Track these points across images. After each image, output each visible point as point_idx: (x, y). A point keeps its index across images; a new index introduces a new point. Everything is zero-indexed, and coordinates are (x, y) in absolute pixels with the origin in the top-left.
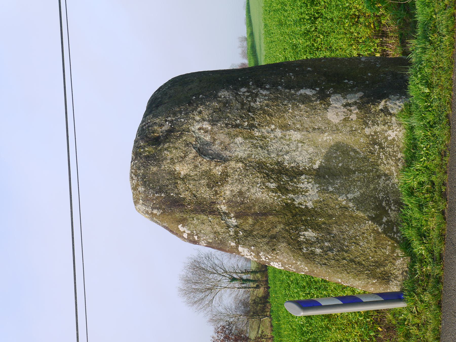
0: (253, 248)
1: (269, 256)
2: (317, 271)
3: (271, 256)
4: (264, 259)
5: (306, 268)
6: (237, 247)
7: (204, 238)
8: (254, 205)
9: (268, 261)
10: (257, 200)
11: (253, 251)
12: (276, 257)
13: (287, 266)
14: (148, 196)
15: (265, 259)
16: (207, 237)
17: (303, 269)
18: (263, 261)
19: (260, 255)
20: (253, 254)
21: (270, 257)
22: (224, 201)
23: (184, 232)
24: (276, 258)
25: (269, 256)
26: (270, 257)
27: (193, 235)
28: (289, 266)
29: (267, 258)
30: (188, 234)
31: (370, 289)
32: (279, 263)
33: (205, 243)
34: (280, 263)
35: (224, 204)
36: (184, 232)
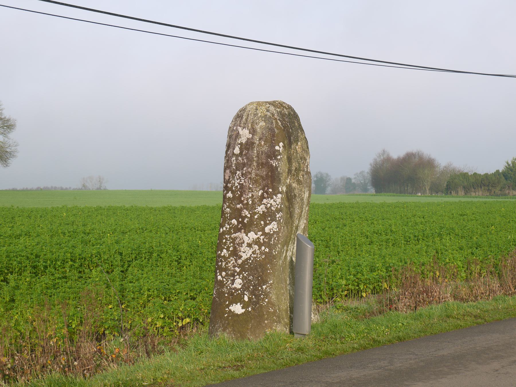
0: (282, 206)
1: (282, 220)
2: (276, 262)
3: (282, 222)
4: (278, 216)
5: (276, 253)
6: (280, 193)
7: (280, 165)
8: (292, 208)
9: (278, 219)
10: (294, 209)
11: (281, 207)
12: (282, 226)
13: (275, 236)
14: (285, 117)
15: (279, 217)
16: (280, 167)
17: (275, 250)
18: (276, 215)
19: (280, 212)
20: (279, 207)
21: (281, 221)
22: (291, 182)
23: (280, 147)
24: (281, 226)
25: (282, 220)
26: (281, 221)
27: (280, 155)
28: (275, 238)
29: (280, 218)
30: (279, 150)
31: (271, 309)
32: (277, 229)
33: (276, 164)
34: (278, 230)
35: (290, 181)
36: (280, 147)
